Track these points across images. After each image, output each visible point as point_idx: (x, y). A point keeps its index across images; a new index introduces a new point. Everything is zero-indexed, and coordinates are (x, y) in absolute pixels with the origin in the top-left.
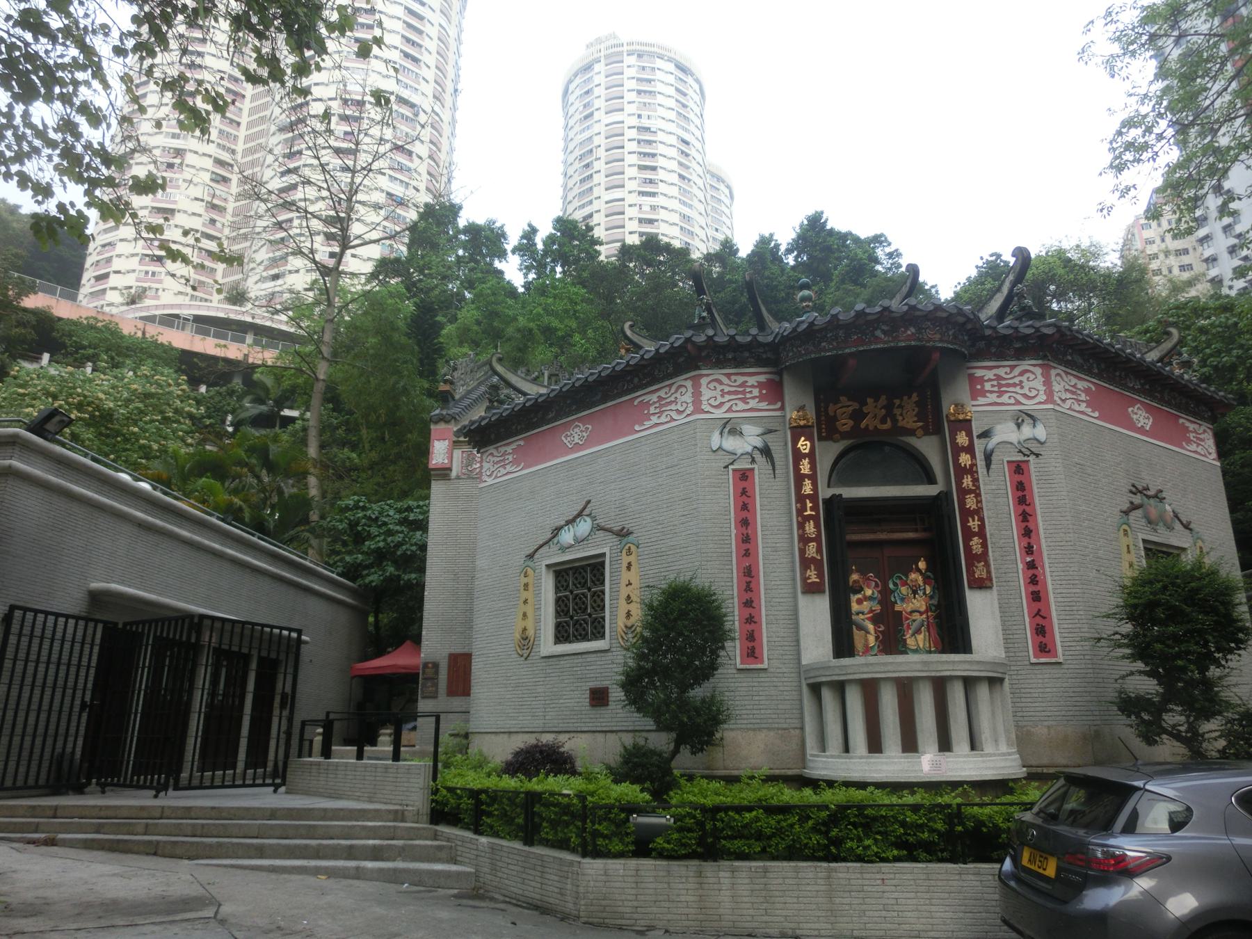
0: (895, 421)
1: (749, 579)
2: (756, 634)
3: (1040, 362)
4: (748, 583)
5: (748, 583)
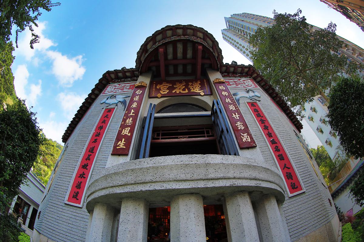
0: (189, 90)
1: (90, 153)
2: (82, 185)
3: (249, 78)
4: (89, 155)
5: (89, 155)
